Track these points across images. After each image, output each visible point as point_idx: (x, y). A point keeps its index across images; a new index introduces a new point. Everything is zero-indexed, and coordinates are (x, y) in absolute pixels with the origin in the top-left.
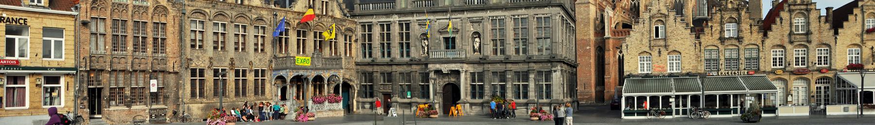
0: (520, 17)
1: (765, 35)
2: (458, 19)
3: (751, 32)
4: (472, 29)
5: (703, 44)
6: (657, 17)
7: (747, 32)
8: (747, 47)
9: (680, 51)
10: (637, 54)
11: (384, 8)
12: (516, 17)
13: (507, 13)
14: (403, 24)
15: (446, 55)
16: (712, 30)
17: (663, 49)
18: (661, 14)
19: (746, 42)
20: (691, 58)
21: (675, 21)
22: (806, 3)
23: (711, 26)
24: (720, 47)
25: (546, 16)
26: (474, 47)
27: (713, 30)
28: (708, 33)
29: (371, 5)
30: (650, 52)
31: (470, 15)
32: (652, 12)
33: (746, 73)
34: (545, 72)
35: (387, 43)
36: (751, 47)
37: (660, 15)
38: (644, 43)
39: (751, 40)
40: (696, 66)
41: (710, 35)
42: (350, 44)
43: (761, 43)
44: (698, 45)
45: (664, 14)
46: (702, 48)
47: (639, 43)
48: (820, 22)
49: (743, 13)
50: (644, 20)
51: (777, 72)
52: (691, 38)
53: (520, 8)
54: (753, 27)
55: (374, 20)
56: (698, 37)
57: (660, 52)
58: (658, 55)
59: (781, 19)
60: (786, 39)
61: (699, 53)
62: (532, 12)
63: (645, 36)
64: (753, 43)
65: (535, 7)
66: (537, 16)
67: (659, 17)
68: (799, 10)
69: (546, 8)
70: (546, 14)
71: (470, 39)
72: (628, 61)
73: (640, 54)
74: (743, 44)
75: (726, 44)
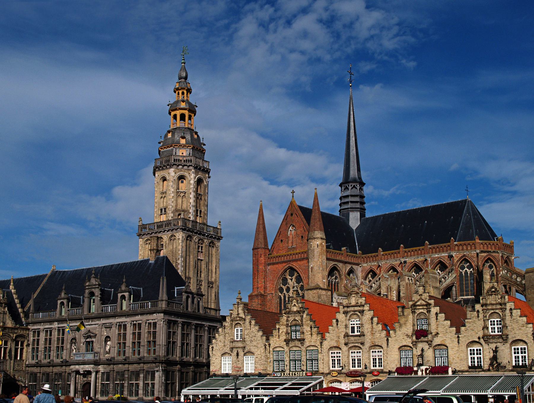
1: (323, 338)
2: (97, 325)
3: (311, 334)
4: (105, 334)
5: (271, 345)
7: (308, 334)
8: (309, 349)
11: (49, 317)
14: (60, 329)
16: (279, 332)
19: (307, 344)
21: (250, 324)
22: (359, 304)
23: (279, 329)
24: (285, 348)
25: (154, 321)
27: (280, 332)
28: (276, 335)
29: (41, 313)
33: (304, 375)
35: (49, 347)
36: (312, 348)
39: (311, 342)
41: (277, 337)
42: (22, 350)
43: (320, 345)
44: (267, 347)
46: (270, 349)
48: (372, 323)
49: (305, 316)
51: (333, 374)
53: (137, 315)
54: (313, 329)
55: (41, 327)
56: (268, 339)
59: (337, 321)
60: (342, 341)
61: (268, 354)
62: (145, 318)
64: (312, 344)
65: (147, 314)
66: (148, 322)
68: (353, 311)
69: (154, 314)
70: (155, 320)
71: (103, 343)
73: (222, 355)
74: (304, 346)
75: (290, 346)
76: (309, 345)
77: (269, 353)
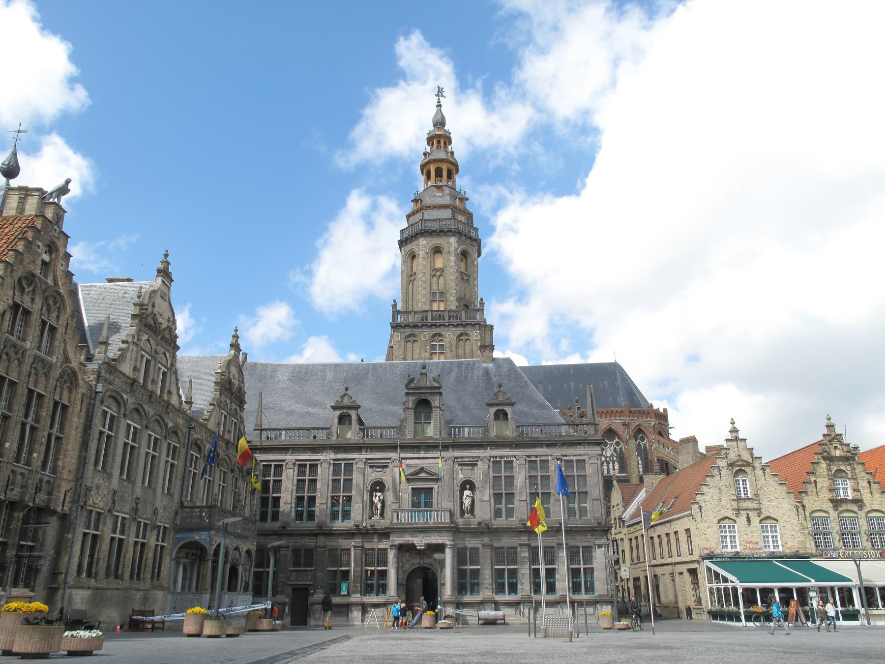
0: (538, 459)
4: (461, 476)
5: (807, 507)
6: (737, 466)
9: (776, 517)
10: (716, 521)
12: (533, 458)
13: (518, 452)
15: (421, 517)
17: (753, 515)
18: (742, 461)
20: (793, 530)
21: (764, 473)
23: (815, 482)
26: (462, 503)
27: (818, 487)
30: (734, 517)
31: (458, 453)
32: (729, 458)
34: (583, 547)
37: (740, 463)
38: (723, 503)
40: (803, 542)
41: (814, 494)
44: (800, 510)
45: (746, 461)
46: (806, 514)
47: (716, 503)
50: (720, 470)
52: (790, 497)
54: (872, 485)
57: (748, 519)
58: (746, 523)
61: (804, 522)
63: (723, 494)
64: (876, 508)
67: (740, 466)
72: (705, 532)
76: (870, 509)
77: (805, 519)
